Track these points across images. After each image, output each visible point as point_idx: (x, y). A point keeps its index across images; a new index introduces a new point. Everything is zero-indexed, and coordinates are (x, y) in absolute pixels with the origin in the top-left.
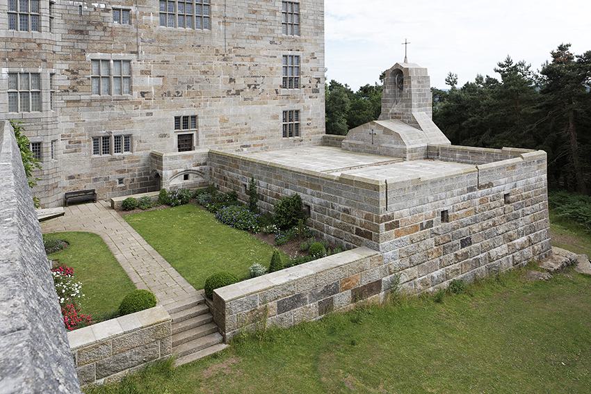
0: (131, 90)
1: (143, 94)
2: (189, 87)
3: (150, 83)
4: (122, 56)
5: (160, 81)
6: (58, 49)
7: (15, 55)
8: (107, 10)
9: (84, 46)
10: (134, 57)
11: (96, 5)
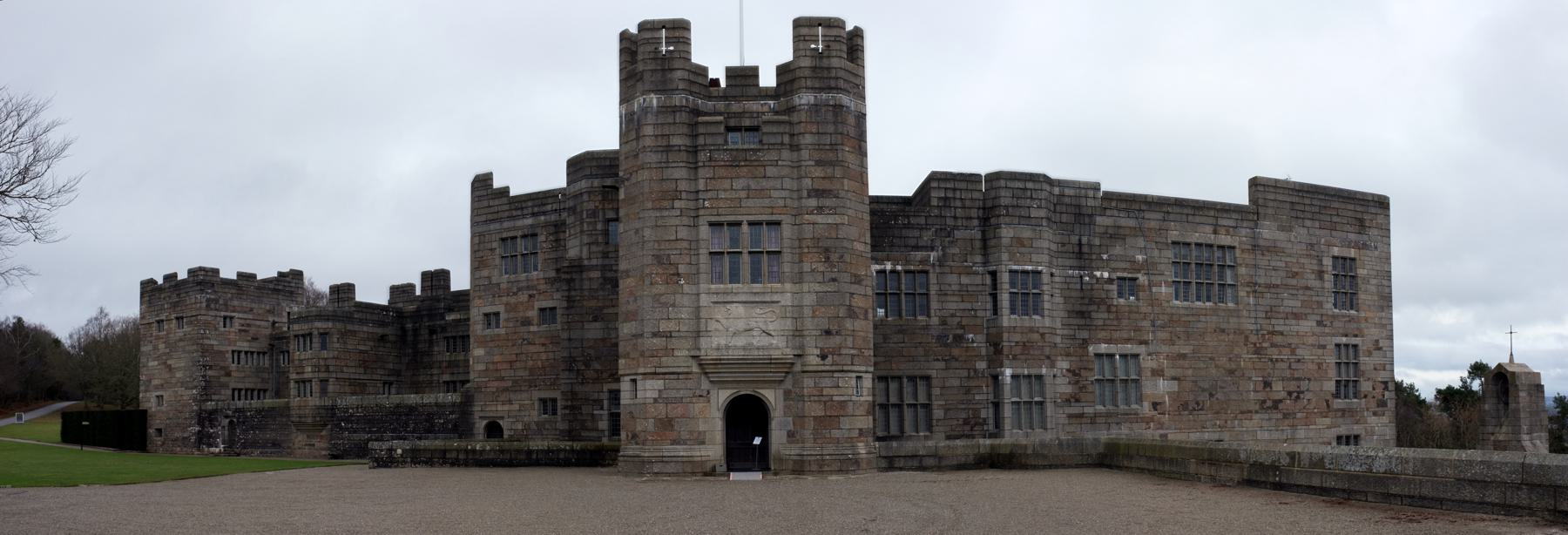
0: (1140, 400)
1: (1155, 405)
2: (1211, 395)
3: (1163, 388)
4: (1130, 348)
5: (1174, 386)
6: (1058, 340)
7: (1018, 350)
8: (1110, 281)
9: (1085, 334)
10: (1141, 350)
11: (1098, 274)
